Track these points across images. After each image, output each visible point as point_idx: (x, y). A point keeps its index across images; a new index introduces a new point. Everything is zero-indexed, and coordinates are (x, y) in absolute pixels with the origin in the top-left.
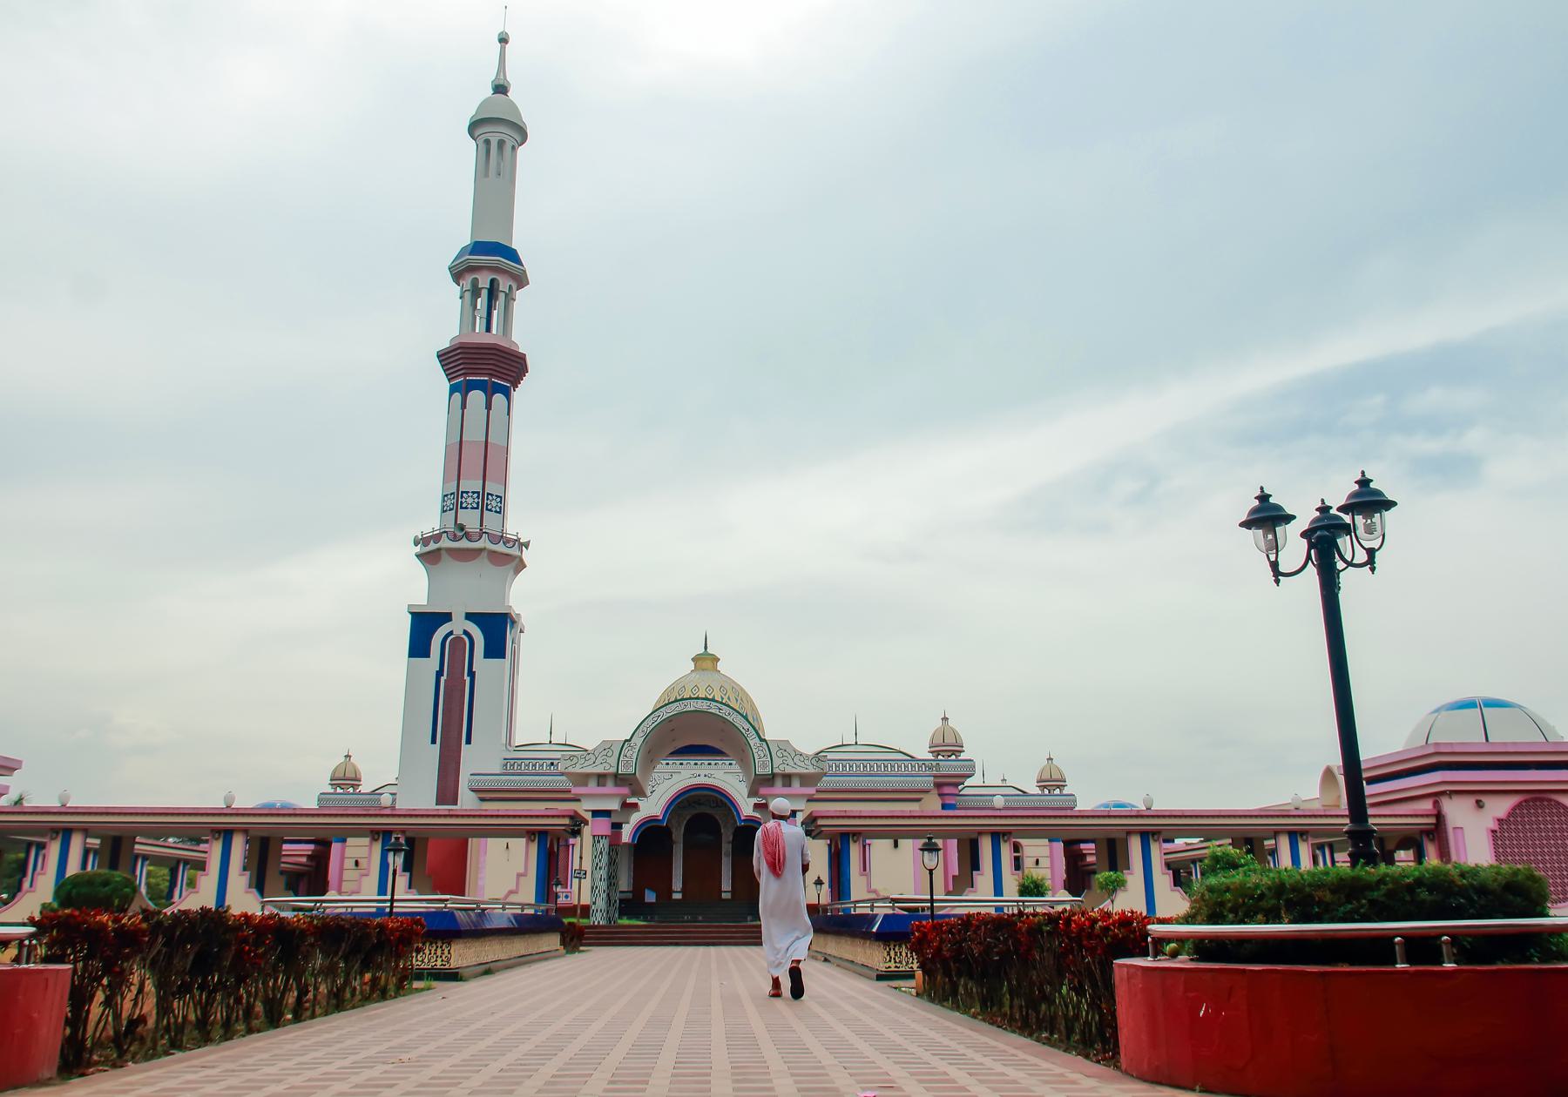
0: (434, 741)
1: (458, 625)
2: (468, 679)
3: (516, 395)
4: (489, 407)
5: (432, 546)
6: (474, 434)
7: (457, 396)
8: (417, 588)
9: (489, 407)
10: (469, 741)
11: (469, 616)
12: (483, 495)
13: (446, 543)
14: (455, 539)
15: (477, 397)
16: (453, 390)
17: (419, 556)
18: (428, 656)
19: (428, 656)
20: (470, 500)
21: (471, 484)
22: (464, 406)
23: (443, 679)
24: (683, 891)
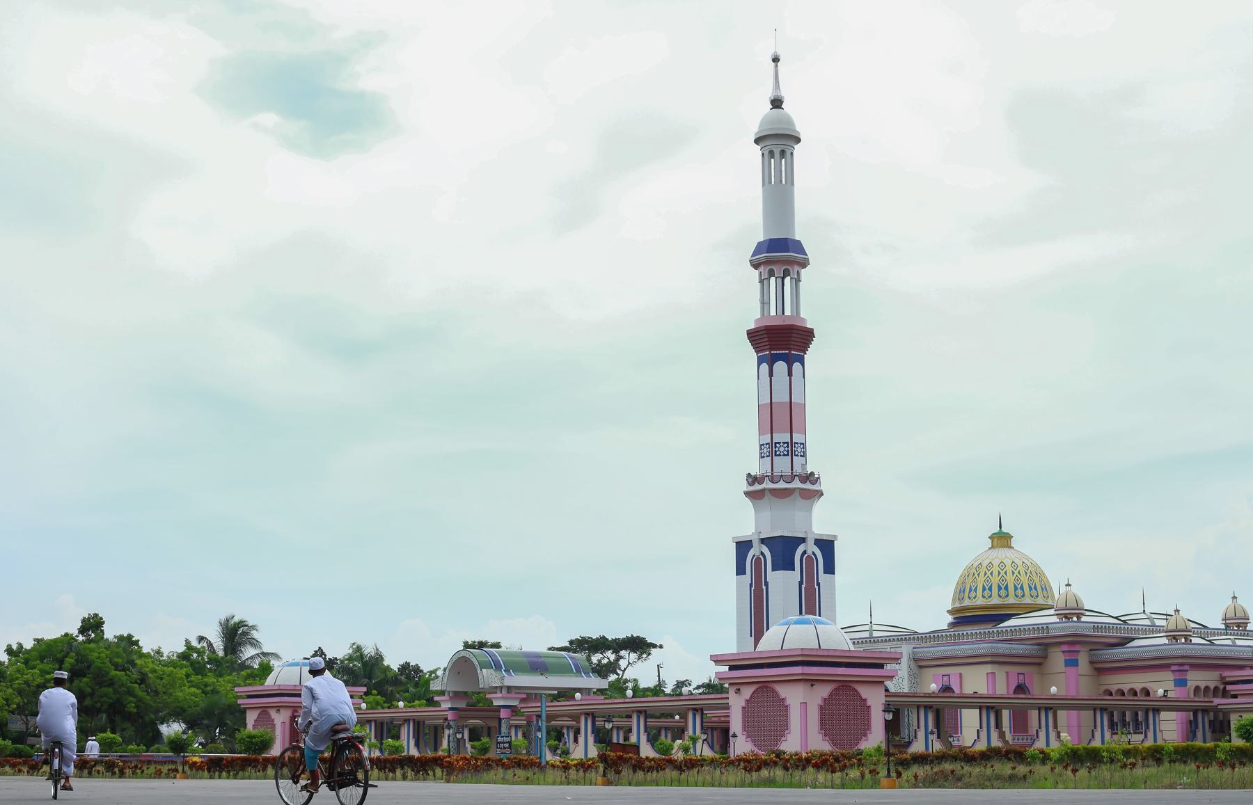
3: (808, 357)
4: (790, 374)
5: (757, 487)
6: (781, 397)
7: (765, 366)
8: (748, 522)
9: (790, 374)
12: (791, 444)
13: (767, 485)
14: (773, 479)
15: (781, 367)
16: (760, 361)
17: (747, 494)
21: (785, 437)
22: (771, 375)
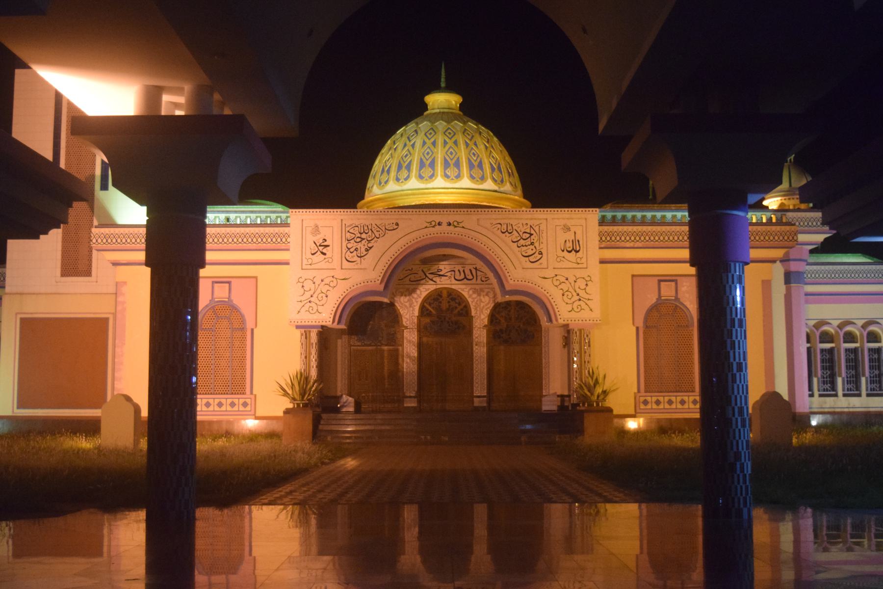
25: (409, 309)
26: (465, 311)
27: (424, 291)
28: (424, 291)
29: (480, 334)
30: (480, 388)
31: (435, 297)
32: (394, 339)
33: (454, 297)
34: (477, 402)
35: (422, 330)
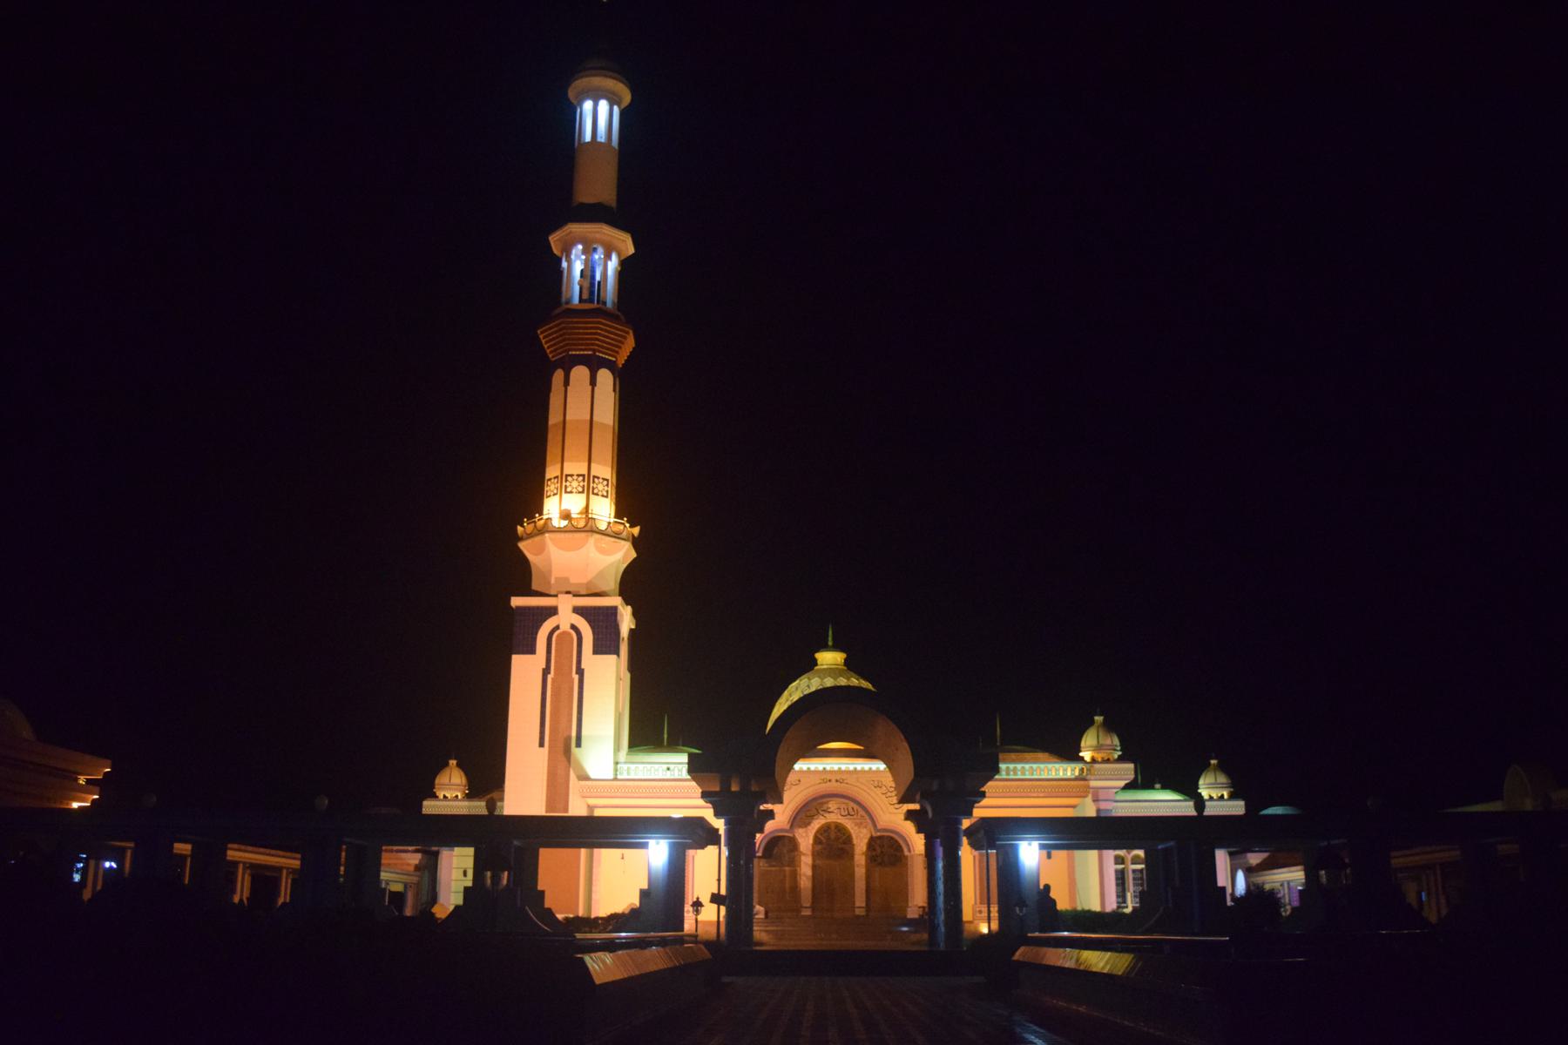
0: (541, 745)
1: (566, 618)
2: (576, 677)
4: (593, 383)
9: (593, 383)
10: (579, 745)
11: (577, 610)
15: (580, 373)
18: (531, 650)
19: (531, 650)
20: (575, 484)
22: (567, 383)
23: (550, 677)
24: (813, 908)
25: (805, 839)
26: (848, 840)
27: (817, 824)
28: (817, 824)
29: (860, 859)
30: (860, 901)
31: (825, 829)
32: (793, 862)
33: (840, 828)
34: (858, 912)
35: (816, 855)
